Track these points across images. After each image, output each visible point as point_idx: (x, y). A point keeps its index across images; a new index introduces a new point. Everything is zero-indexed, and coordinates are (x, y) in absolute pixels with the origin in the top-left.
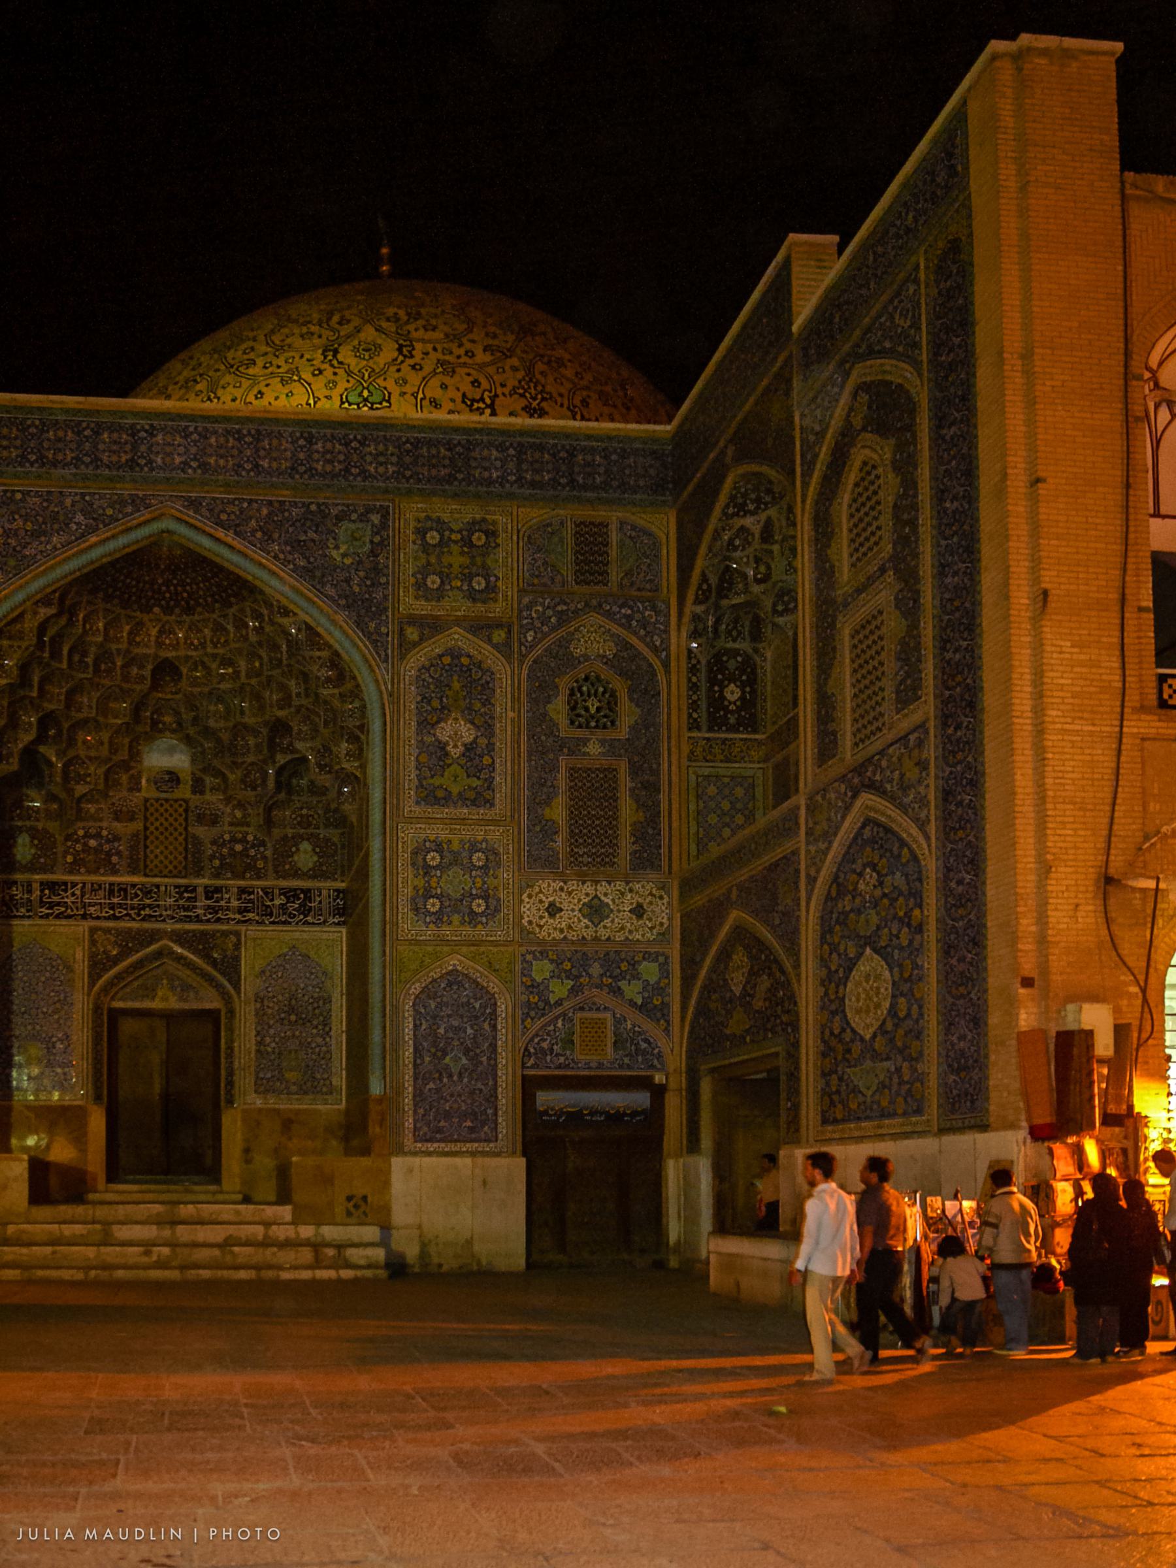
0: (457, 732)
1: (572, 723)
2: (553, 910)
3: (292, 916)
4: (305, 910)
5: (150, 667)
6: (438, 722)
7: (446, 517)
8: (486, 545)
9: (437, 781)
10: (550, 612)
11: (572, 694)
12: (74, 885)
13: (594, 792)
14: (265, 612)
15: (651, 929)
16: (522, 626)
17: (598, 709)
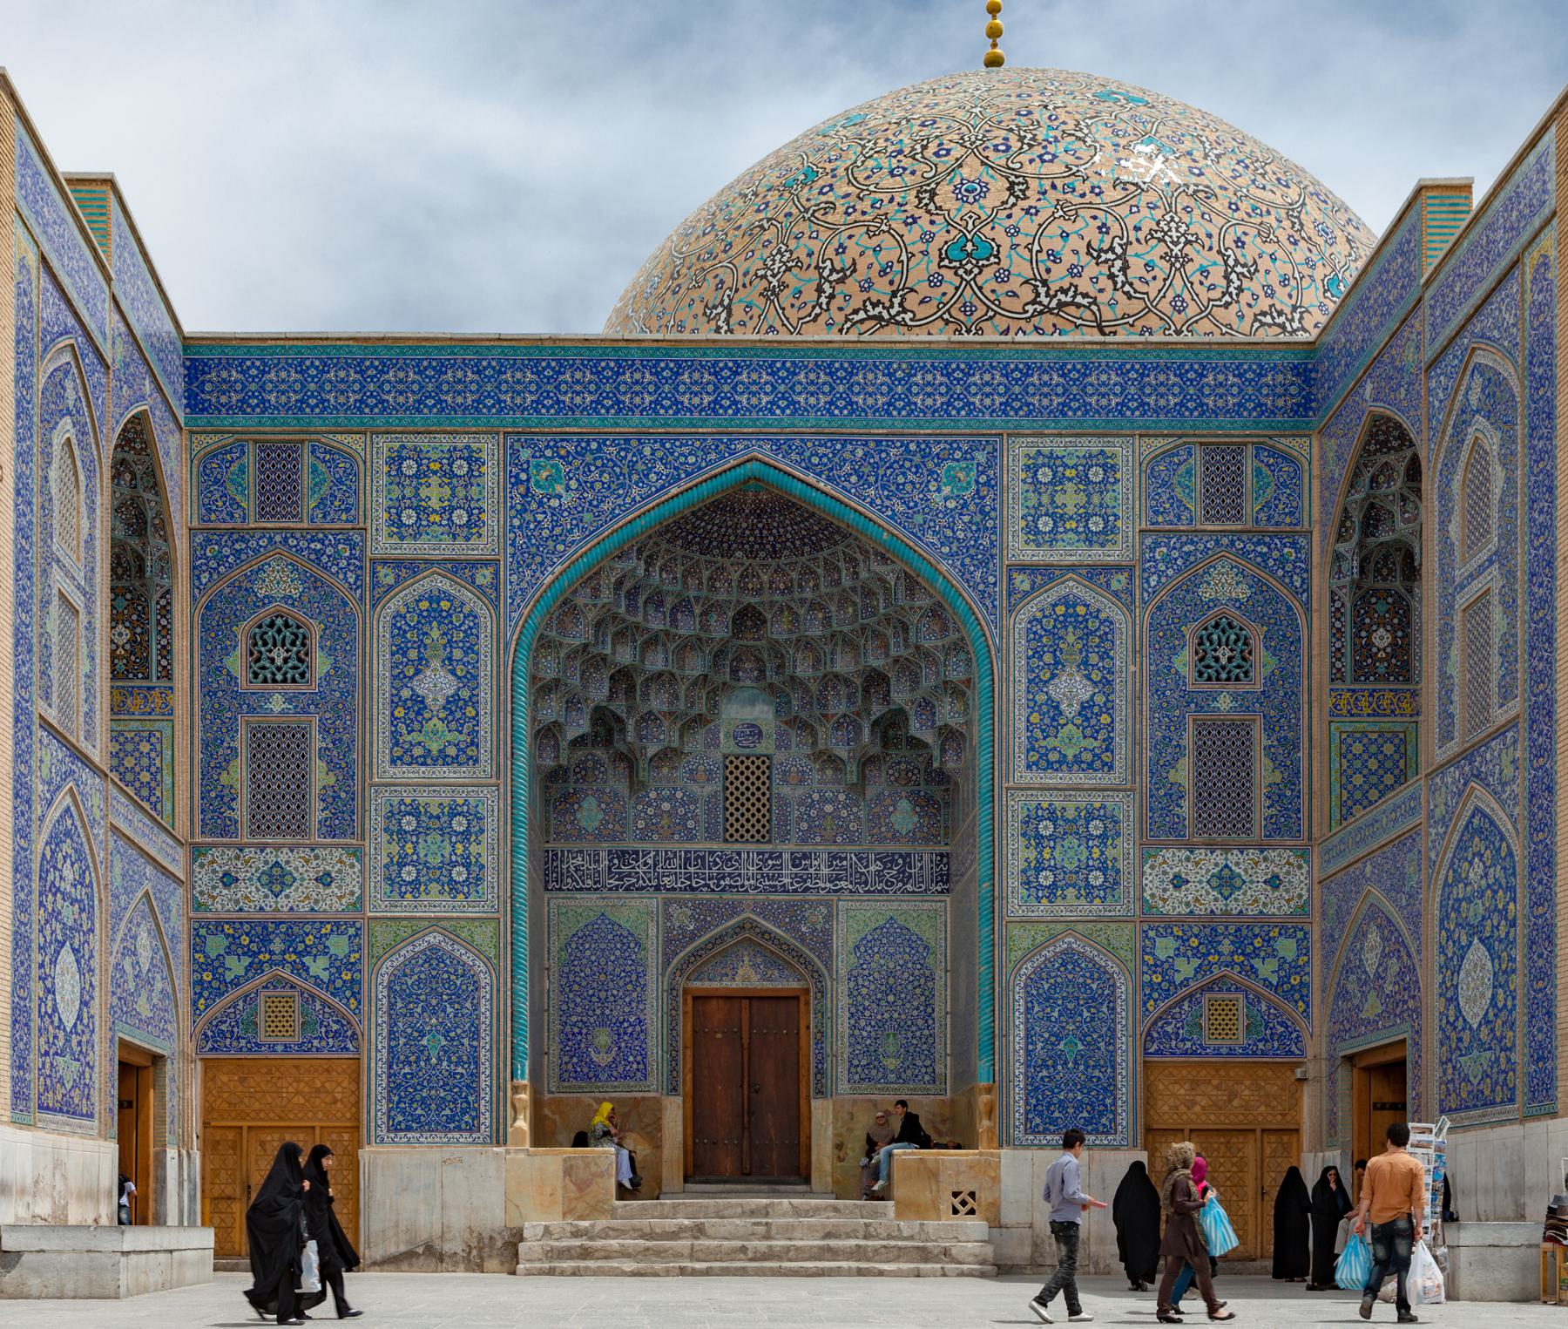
0: (1072, 688)
1: (1201, 674)
2: (1179, 882)
3: (889, 884)
4: (904, 877)
5: (731, 614)
6: (1053, 676)
7: (1059, 452)
8: (1104, 481)
9: (1051, 742)
10: (1175, 554)
11: (1201, 644)
12: (646, 853)
13: (1223, 751)
14: (859, 557)
15: (1288, 901)
16: (1144, 570)
17: (1230, 659)
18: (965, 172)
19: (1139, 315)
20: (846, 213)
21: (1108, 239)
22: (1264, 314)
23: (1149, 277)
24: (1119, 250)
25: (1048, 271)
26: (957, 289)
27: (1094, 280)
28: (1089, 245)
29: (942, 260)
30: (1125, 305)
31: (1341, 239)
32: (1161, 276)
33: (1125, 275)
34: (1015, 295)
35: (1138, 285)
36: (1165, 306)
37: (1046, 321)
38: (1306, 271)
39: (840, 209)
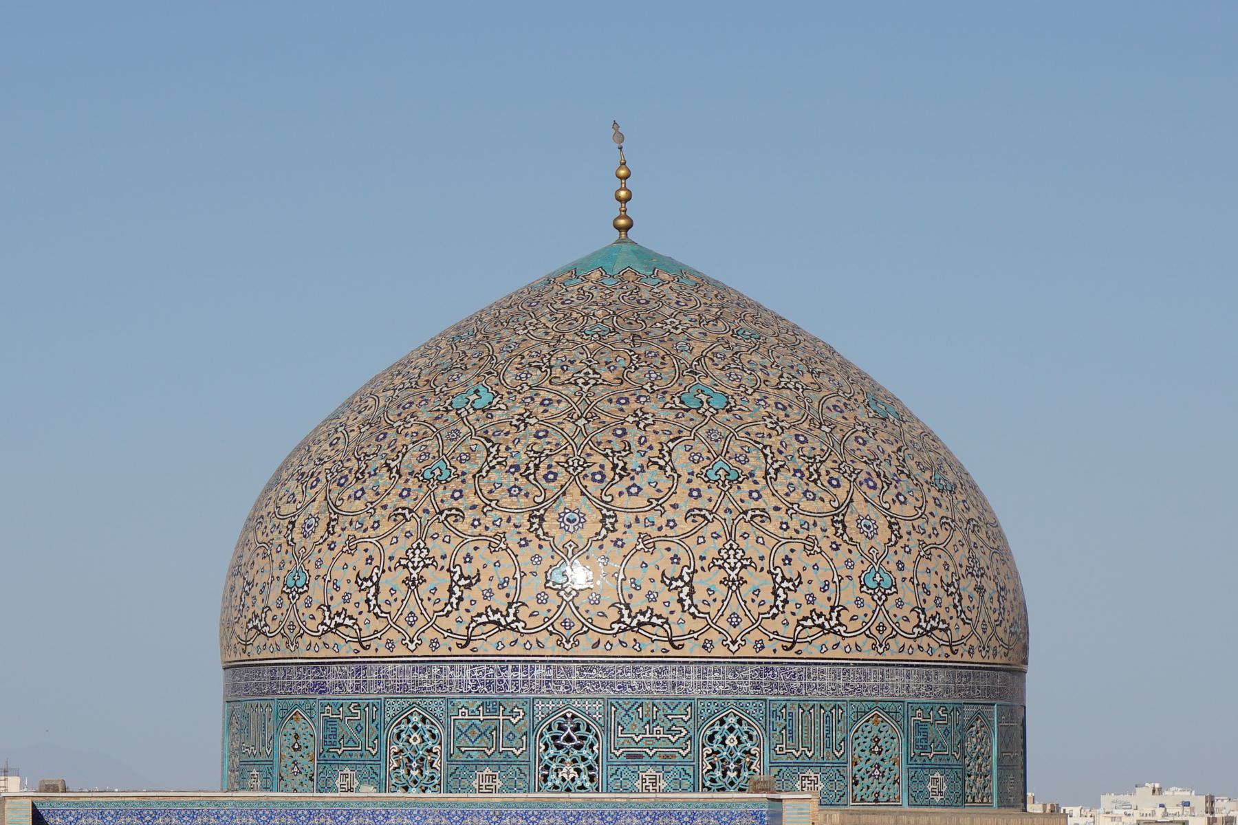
18: (568, 498)
19: (702, 632)
20: (472, 524)
21: (679, 567)
22: (805, 619)
23: (710, 600)
24: (687, 579)
25: (630, 596)
26: (559, 607)
27: (667, 604)
28: (663, 574)
29: (548, 581)
31: (882, 523)
33: (691, 599)
34: (604, 615)
35: (702, 608)
36: (723, 623)
37: (628, 637)
39: (469, 520)
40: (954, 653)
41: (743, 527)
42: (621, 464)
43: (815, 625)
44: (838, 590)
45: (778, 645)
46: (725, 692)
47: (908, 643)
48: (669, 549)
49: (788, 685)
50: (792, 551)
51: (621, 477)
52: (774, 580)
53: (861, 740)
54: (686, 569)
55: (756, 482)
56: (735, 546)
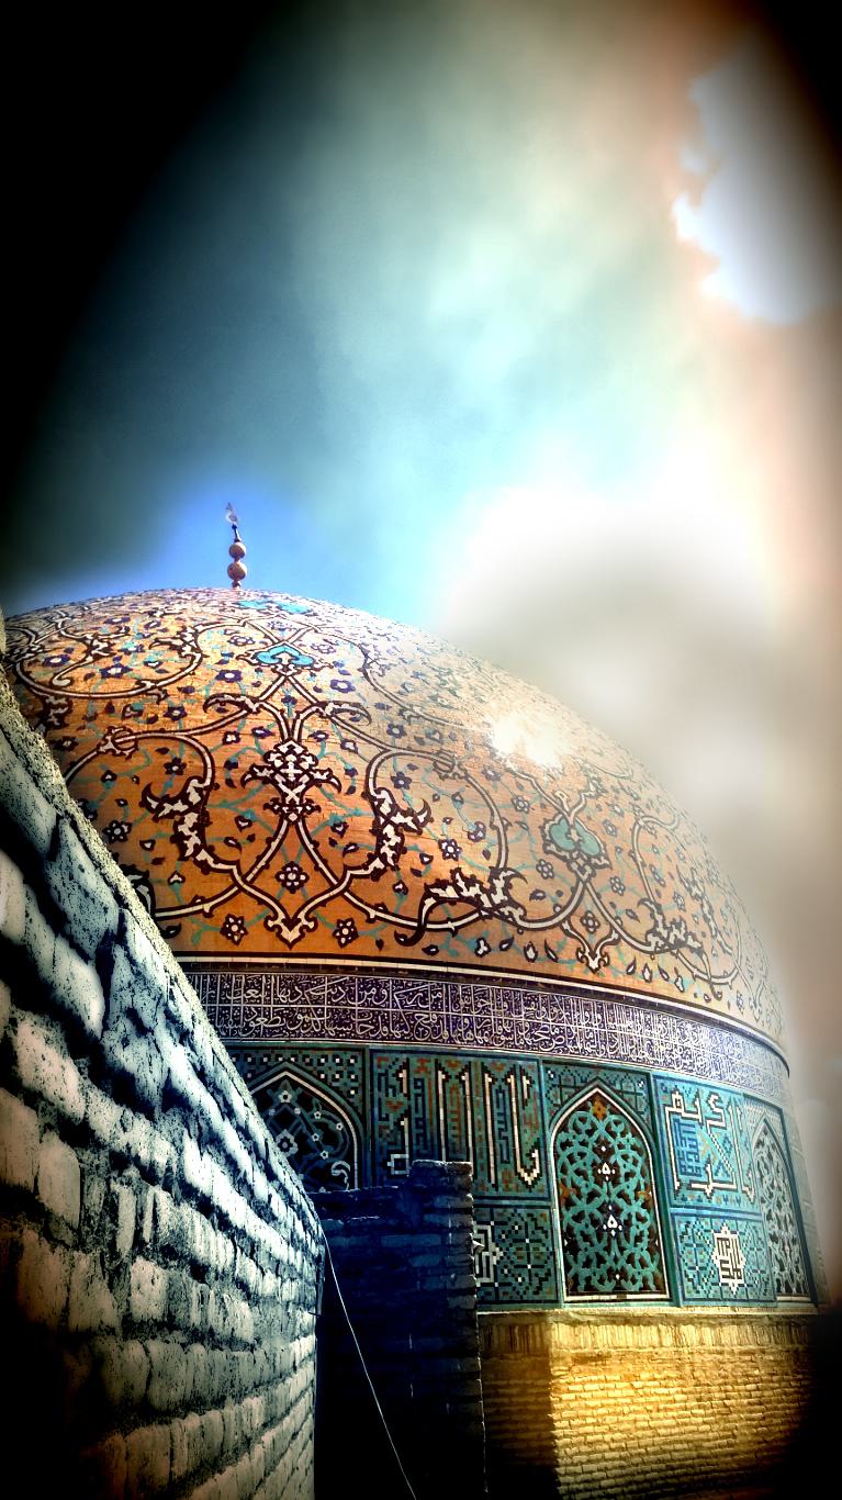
22: (442, 884)
23: (242, 838)
24: (195, 798)
28: (147, 791)
30: (198, 884)
32: (262, 835)
35: (221, 849)
38: (513, 816)
40: (718, 996)
41: (315, 724)
42: (103, 645)
43: (462, 899)
44: (503, 845)
45: (387, 934)
46: (271, 1032)
47: (643, 960)
48: (163, 751)
49: (411, 1017)
50: (412, 768)
51: (97, 657)
52: (376, 810)
53: (575, 1149)
54: (195, 783)
55: (344, 673)
56: (299, 750)
